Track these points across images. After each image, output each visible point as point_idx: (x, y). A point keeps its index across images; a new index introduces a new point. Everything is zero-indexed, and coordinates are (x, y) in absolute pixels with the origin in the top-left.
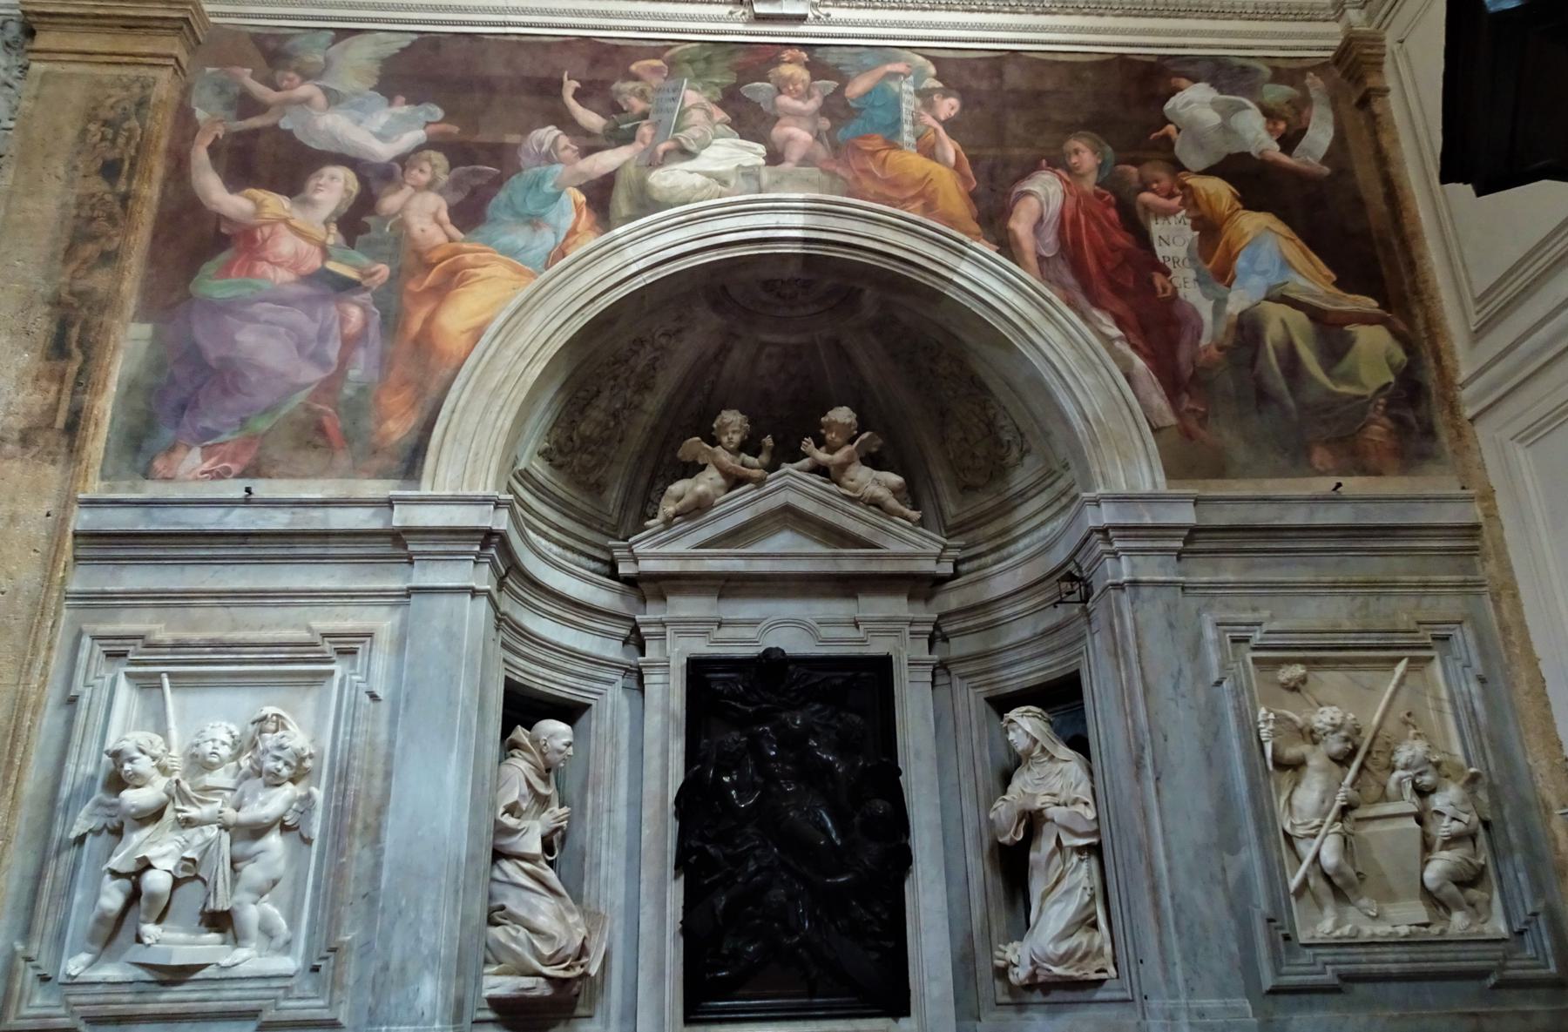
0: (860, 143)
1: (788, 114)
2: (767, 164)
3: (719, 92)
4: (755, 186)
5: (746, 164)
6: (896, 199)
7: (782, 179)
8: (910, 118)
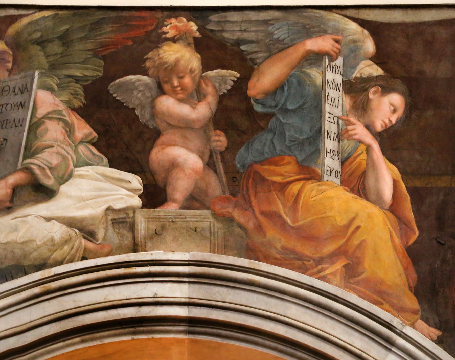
0: (265, 170)
1: (171, 126)
2: (144, 206)
3: (81, 92)
4: (128, 241)
5: (118, 206)
6: (309, 259)
7: (163, 228)
8: (334, 129)
